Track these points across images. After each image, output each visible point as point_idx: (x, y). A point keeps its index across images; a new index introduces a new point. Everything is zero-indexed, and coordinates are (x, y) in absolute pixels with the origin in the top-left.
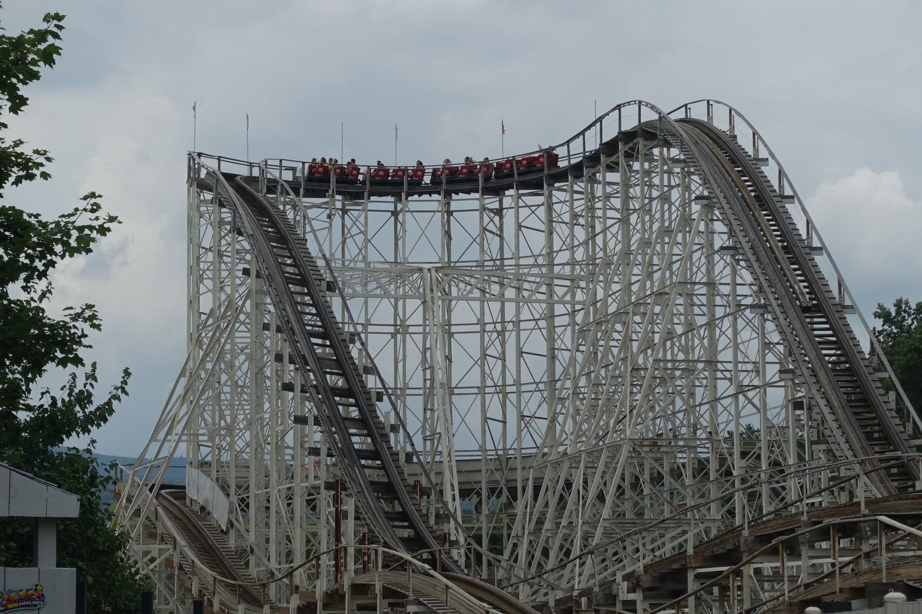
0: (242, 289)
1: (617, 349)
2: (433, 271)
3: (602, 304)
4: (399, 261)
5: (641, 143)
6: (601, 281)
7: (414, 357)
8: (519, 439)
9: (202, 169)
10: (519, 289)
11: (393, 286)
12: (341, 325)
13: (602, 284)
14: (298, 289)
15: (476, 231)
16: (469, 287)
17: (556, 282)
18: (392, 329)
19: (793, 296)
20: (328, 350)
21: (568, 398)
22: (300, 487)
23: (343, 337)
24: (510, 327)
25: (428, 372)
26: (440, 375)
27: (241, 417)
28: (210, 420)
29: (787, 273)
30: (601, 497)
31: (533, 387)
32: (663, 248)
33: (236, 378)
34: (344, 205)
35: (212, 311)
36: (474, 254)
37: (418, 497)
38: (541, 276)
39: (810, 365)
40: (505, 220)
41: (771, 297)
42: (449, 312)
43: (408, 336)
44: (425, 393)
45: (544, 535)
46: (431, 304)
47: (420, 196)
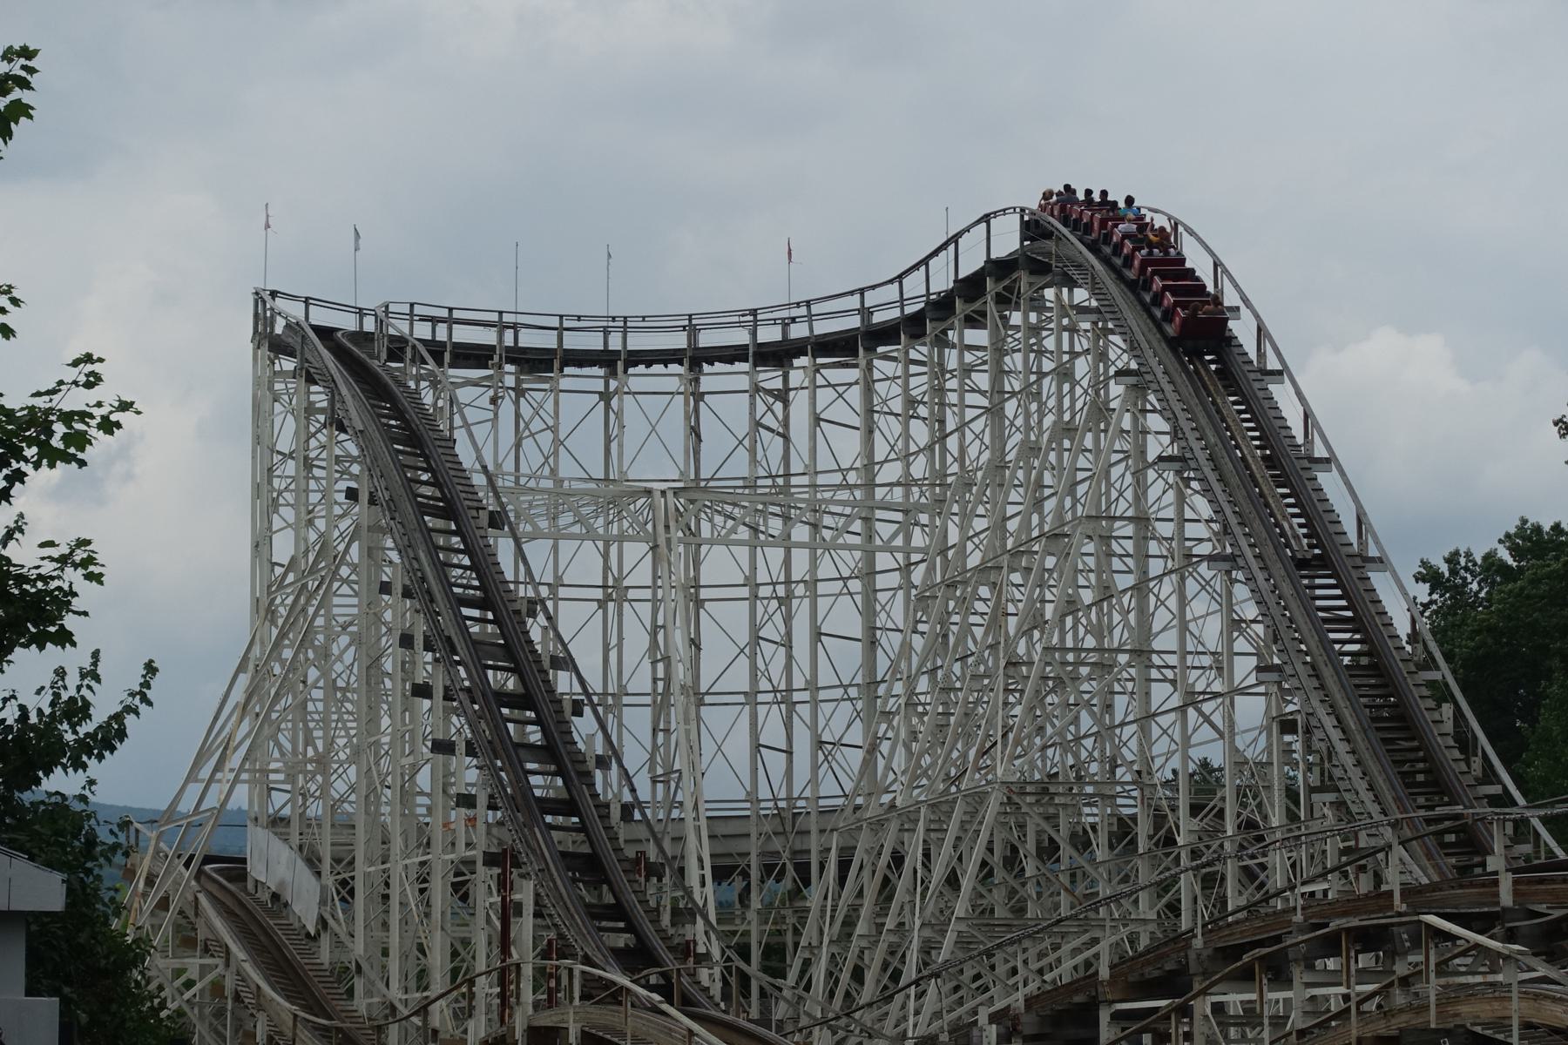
0: (344, 524)
1: (982, 629)
2: (670, 495)
3: (956, 553)
4: (612, 477)
5: (1024, 279)
6: (956, 514)
7: (636, 641)
8: (814, 781)
9: (278, 318)
10: (815, 527)
11: (601, 521)
12: (512, 586)
13: (956, 519)
14: (439, 523)
15: (742, 427)
16: (730, 523)
17: (879, 514)
18: (599, 594)
19: (1280, 540)
20: (490, 628)
21: (898, 712)
22: (441, 861)
23: (517, 606)
24: (800, 590)
25: (660, 666)
26: (680, 673)
27: (341, 742)
28: (288, 746)
29: (1271, 501)
30: (953, 881)
31: (839, 693)
32: (1060, 458)
33: (334, 676)
34: (518, 381)
35: (293, 560)
36: (739, 466)
37: (642, 880)
38: (853, 504)
39: (1308, 659)
40: (792, 408)
41: (1243, 542)
42: (697, 564)
43: (626, 604)
44: (655, 702)
45: (856, 944)
46: (666, 551)
47: (649, 365)
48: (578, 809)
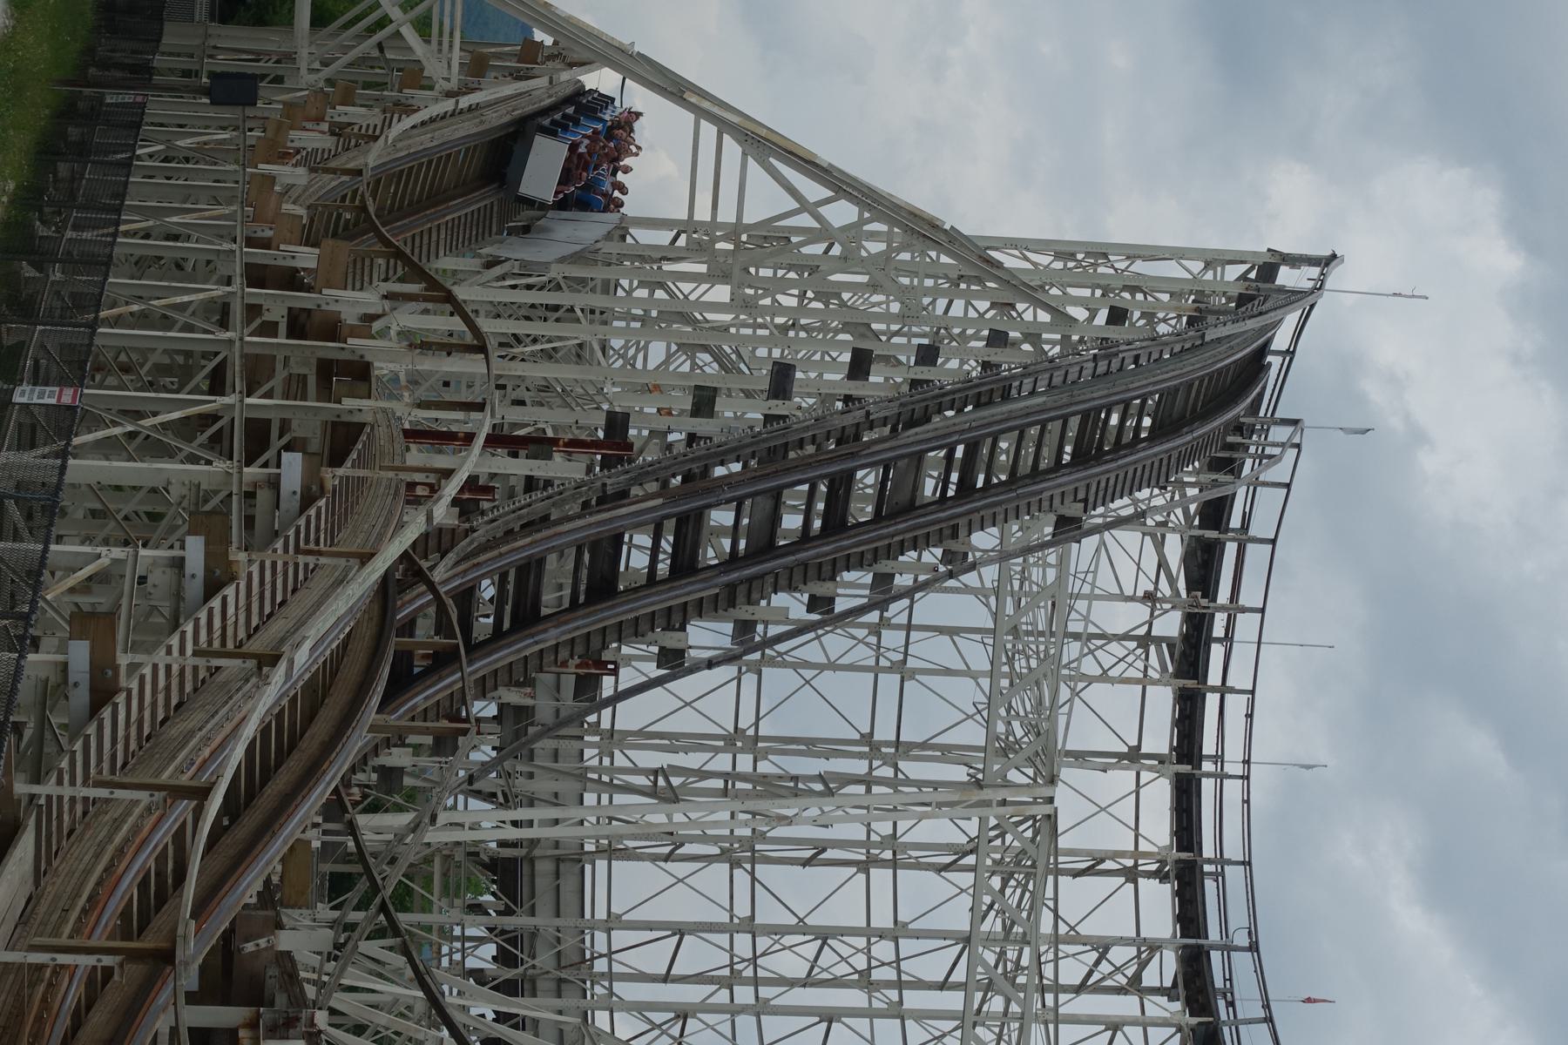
23: (962, 532)
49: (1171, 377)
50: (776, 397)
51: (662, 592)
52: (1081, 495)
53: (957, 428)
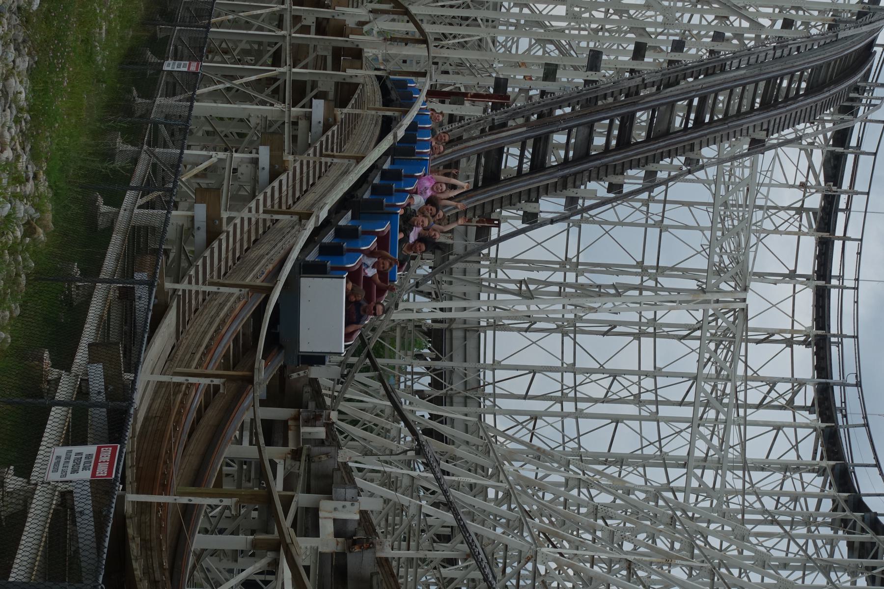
23: (696, 148)
48: (536, 172)
49: (818, 59)
50: (591, 70)
51: (525, 181)
52: (765, 127)
53: (695, 88)
